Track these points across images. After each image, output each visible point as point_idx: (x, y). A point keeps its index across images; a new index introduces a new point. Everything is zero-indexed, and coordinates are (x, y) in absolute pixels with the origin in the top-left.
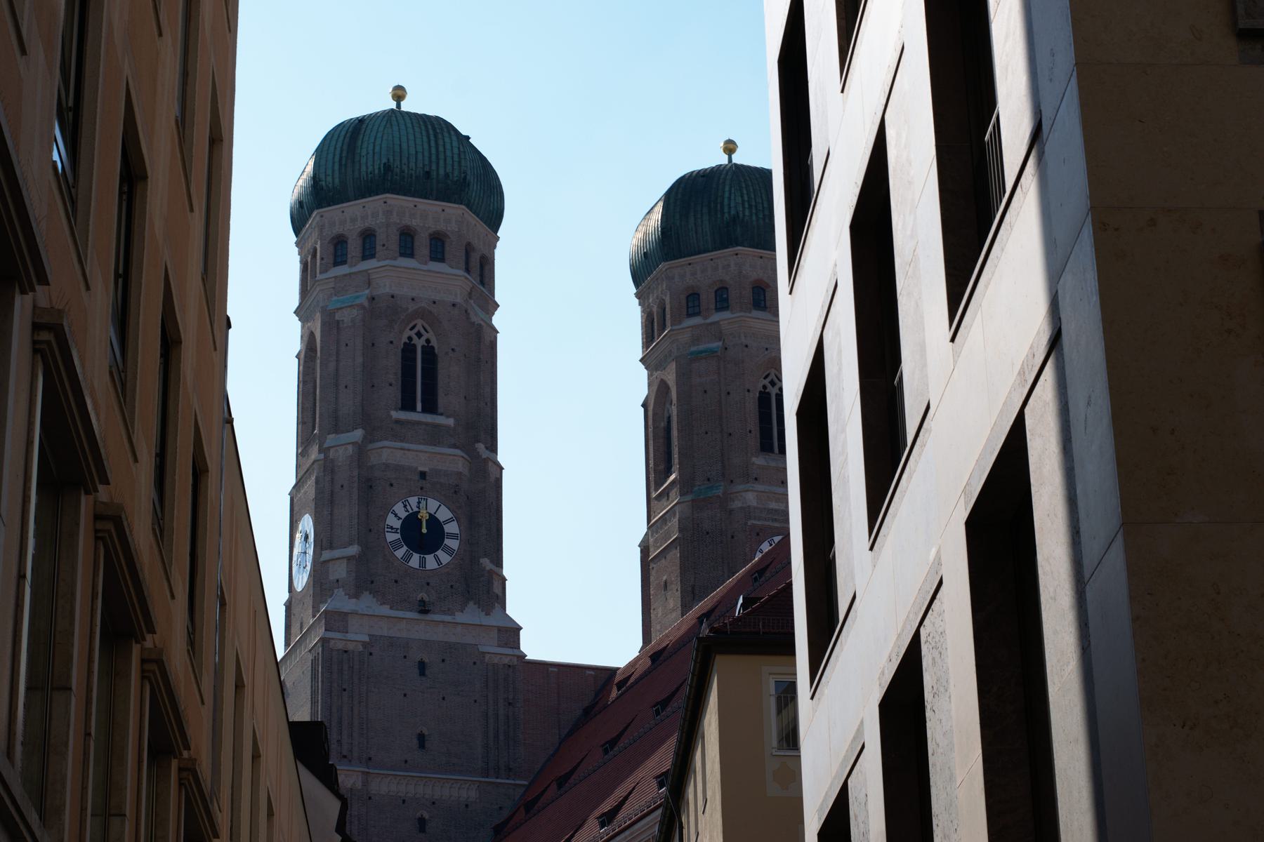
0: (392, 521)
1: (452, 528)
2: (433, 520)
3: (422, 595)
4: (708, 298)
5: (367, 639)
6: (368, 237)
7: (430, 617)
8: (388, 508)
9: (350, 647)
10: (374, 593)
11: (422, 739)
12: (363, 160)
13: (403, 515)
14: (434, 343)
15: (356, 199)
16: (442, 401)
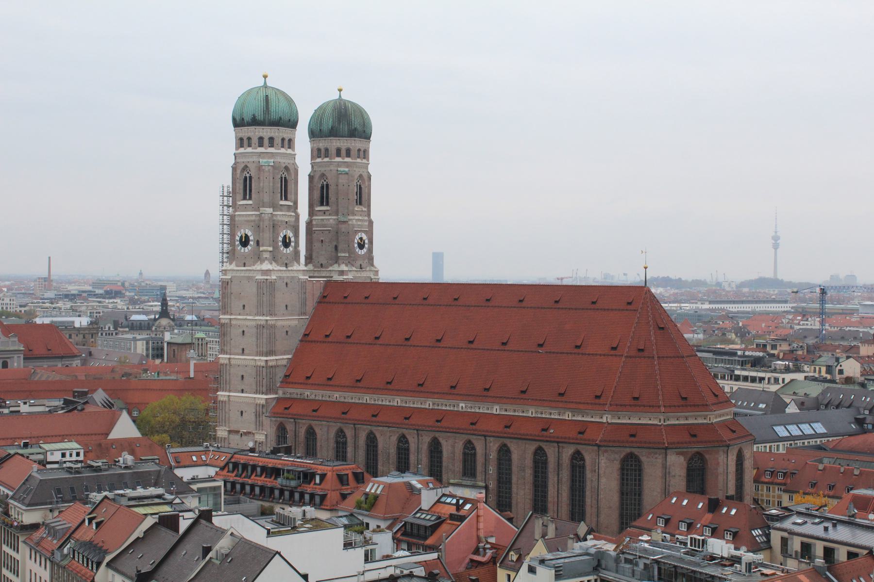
0: (280, 239)
1: (293, 239)
2: (290, 238)
3: (286, 262)
4: (343, 152)
5: (274, 277)
6: (271, 139)
7: (290, 268)
8: (278, 234)
9: (273, 281)
10: (275, 261)
11: (286, 306)
12: (272, 114)
13: (282, 236)
14: (287, 176)
15: (268, 126)
16: (289, 196)
